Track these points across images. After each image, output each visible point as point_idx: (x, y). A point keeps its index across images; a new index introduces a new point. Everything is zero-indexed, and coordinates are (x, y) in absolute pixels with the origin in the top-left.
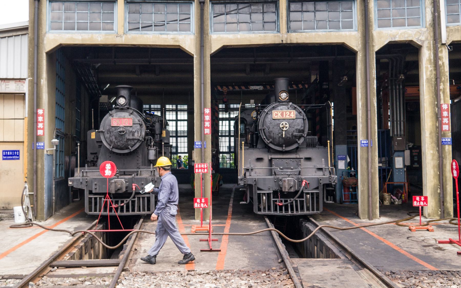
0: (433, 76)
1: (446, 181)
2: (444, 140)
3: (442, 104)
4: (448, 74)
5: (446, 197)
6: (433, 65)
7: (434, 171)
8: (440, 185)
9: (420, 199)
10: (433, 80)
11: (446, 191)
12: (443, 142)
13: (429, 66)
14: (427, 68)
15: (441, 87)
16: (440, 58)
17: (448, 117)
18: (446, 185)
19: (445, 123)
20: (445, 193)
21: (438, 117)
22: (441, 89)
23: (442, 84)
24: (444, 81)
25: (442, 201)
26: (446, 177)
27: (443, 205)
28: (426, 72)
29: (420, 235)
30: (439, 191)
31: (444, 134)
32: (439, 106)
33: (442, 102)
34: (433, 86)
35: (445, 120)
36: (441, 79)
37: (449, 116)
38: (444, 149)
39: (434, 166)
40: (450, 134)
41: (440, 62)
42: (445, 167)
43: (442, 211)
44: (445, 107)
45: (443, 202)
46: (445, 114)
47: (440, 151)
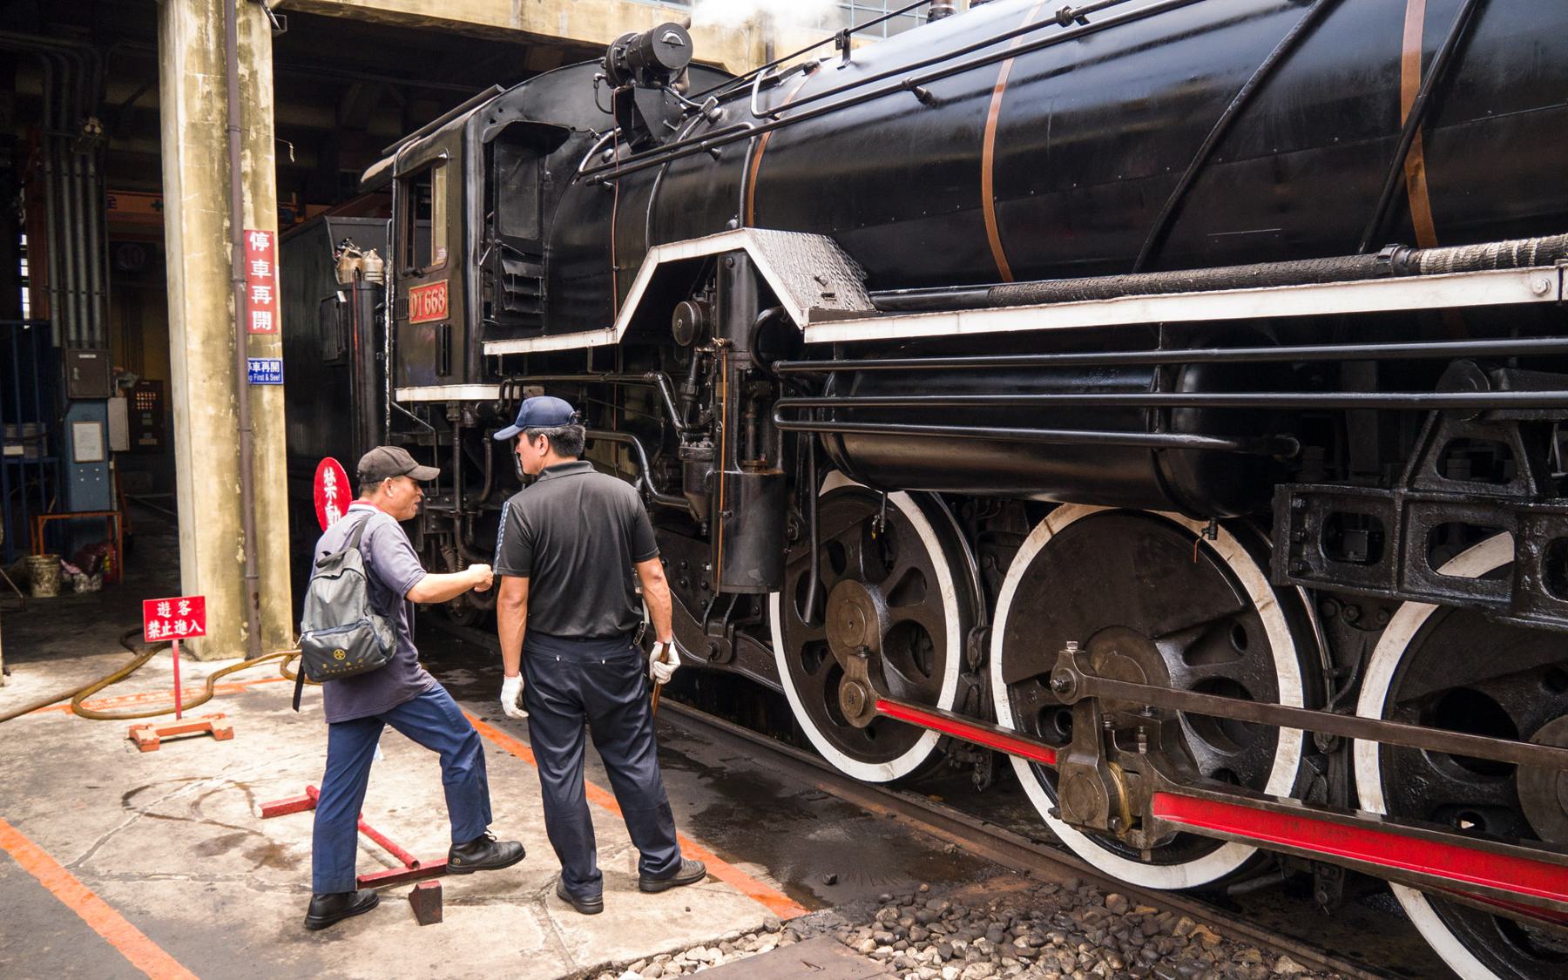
0: (215, 117)
1: (265, 517)
2: (256, 367)
3: (248, 232)
4: (269, 119)
5: (267, 577)
6: (214, 76)
7: (223, 484)
8: (244, 535)
9: (174, 609)
10: (217, 133)
11: (266, 553)
12: (252, 373)
13: (200, 76)
14: (191, 83)
15: (247, 165)
16: (246, 54)
17: (268, 281)
18: (266, 532)
19: (261, 302)
20: (261, 561)
21: (234, 278)
22: (245, 174)
23: (248, 153)
24: (256, 141)
25: (252, 592)
26: (265, 505)
27: (257, 606)
28: (189, 99)
29: (179, 770)
30: (240, 557)
31: (257, 343)
32: (237, 237)
33: (249, 223)
34: (217, 156)
35: (261, 293)
36: (244, 132)
37: (273, 278)
38: (258, 400)
39: (220, 463)
40: (277, 346)
41: (242, 70)
42: (262, 469)
43: (255, 629)
44: (259, 242)
45: (257, 596)
46: (260, 268)
47: (244, 407)
